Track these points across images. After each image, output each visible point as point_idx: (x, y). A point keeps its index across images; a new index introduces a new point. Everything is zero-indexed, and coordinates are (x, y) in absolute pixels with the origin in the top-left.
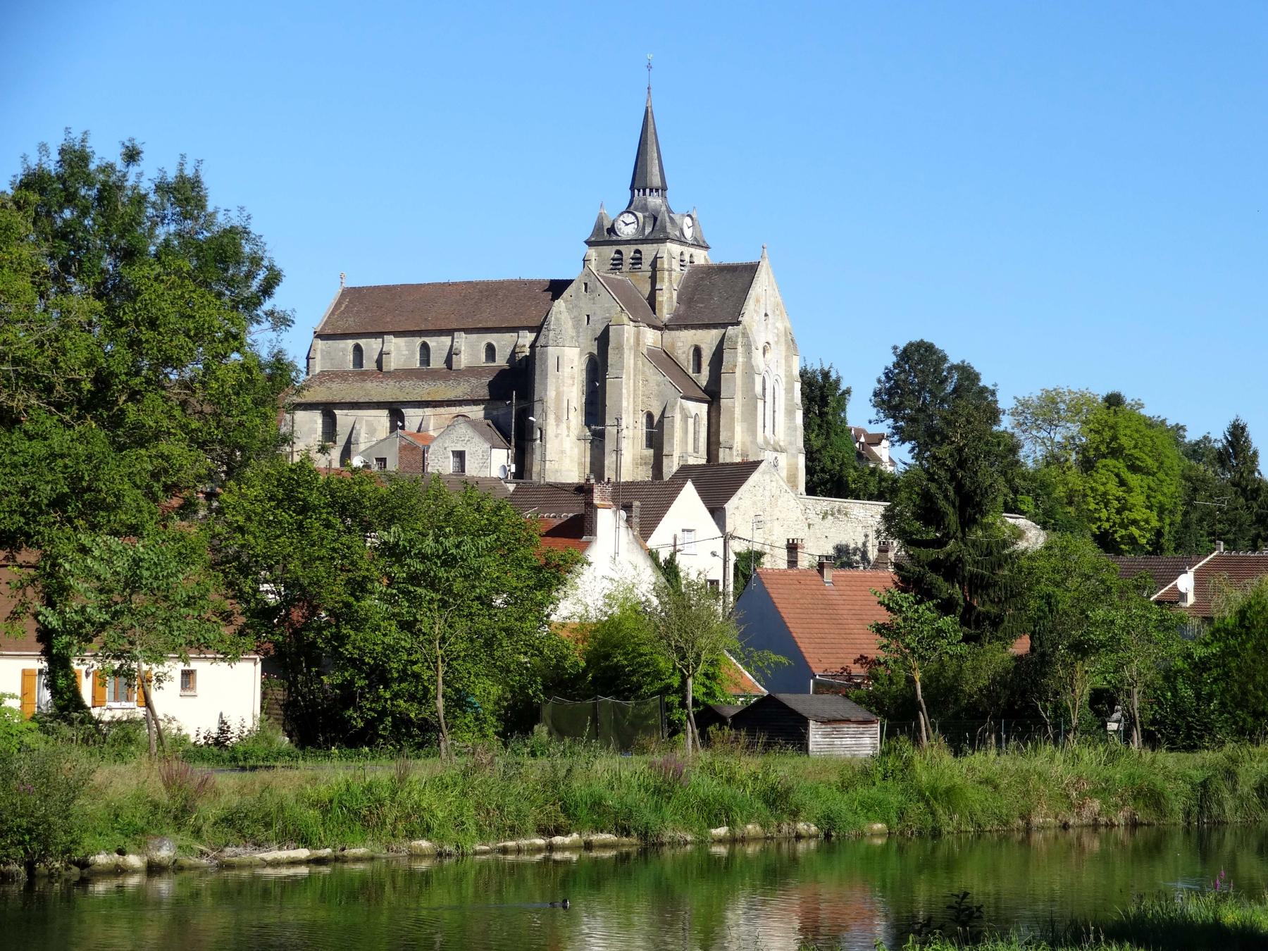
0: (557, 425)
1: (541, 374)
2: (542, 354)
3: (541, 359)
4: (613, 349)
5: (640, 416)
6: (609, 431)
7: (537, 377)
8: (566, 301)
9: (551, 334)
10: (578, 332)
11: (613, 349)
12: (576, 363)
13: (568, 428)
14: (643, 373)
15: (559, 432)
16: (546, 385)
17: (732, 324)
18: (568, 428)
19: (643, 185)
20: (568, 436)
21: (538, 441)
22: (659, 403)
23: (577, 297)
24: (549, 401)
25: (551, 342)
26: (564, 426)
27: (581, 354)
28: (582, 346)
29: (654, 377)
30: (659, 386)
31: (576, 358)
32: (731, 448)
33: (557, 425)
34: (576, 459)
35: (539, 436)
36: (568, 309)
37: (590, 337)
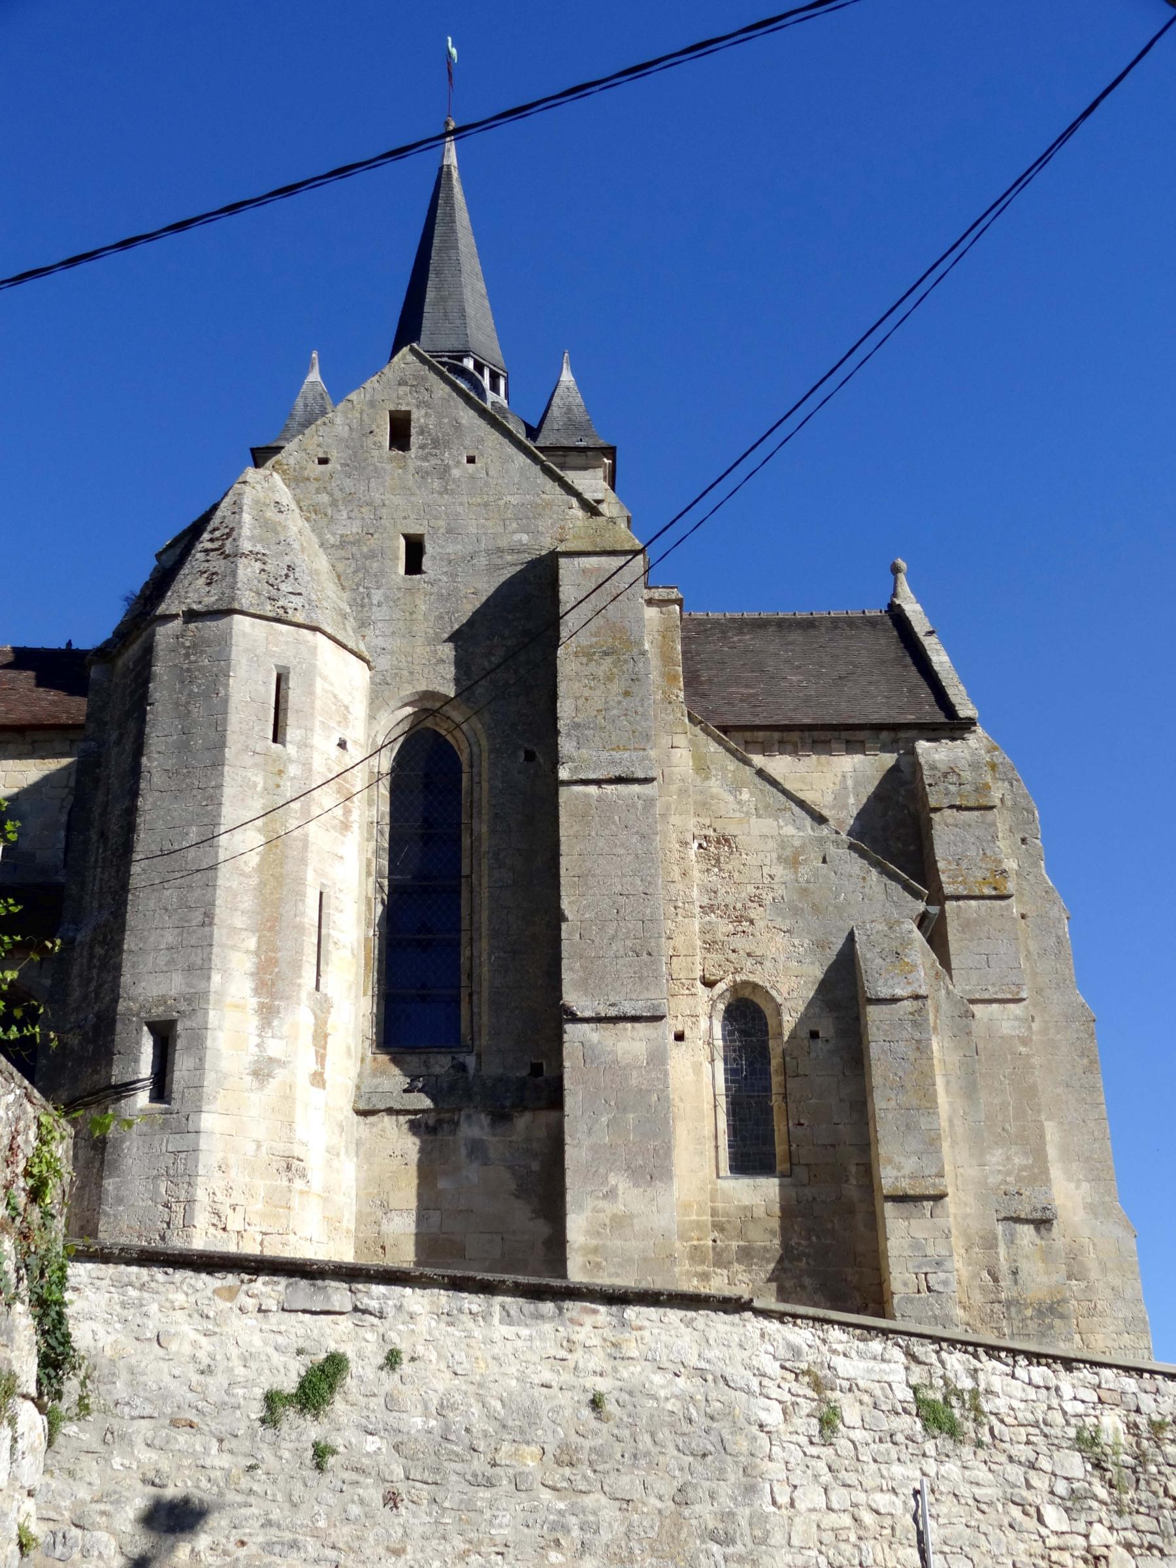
0: (268, 1014)
1: (184, 747)
2: (196, 647)
3: (185, 677)
4: (587, 654)
5: (703, 1008)
6: (589, 1054)
7: (154, 762)
8: (295, 480)
9: (247, 570)
10: (360, 603)
11: (587, 654)
12: (358, 732)
13: (321, 1038)
14: (704, 806)
15: (275, 1048)
16: (212, 799)
17: (933, 732)
18: (321, 1038)
19: (450, 343)
20: (318, 1079)
21: (142, 1099)
22: (802, 943)
23: (357, 463)
24: (226, 879)
25: (246, 599)
26: (301, 1017)
27: (377, 699)
28: (383, 663)
29: (766, 825)
30: (793, 862)
31: (359, 707)
32: (1042, 1223)
33: (268, 1014)
34: (349, 1223)
35: (146, 1068)
36: (311, 512)
37: (424, 628)
